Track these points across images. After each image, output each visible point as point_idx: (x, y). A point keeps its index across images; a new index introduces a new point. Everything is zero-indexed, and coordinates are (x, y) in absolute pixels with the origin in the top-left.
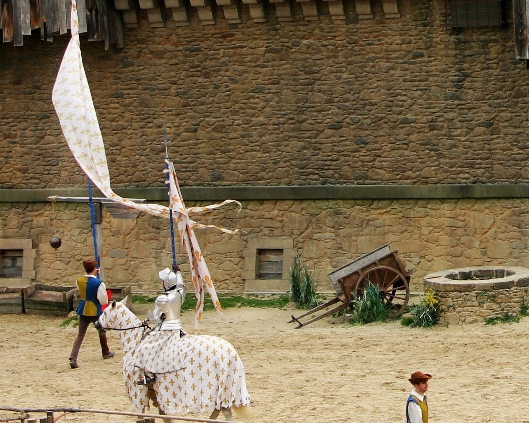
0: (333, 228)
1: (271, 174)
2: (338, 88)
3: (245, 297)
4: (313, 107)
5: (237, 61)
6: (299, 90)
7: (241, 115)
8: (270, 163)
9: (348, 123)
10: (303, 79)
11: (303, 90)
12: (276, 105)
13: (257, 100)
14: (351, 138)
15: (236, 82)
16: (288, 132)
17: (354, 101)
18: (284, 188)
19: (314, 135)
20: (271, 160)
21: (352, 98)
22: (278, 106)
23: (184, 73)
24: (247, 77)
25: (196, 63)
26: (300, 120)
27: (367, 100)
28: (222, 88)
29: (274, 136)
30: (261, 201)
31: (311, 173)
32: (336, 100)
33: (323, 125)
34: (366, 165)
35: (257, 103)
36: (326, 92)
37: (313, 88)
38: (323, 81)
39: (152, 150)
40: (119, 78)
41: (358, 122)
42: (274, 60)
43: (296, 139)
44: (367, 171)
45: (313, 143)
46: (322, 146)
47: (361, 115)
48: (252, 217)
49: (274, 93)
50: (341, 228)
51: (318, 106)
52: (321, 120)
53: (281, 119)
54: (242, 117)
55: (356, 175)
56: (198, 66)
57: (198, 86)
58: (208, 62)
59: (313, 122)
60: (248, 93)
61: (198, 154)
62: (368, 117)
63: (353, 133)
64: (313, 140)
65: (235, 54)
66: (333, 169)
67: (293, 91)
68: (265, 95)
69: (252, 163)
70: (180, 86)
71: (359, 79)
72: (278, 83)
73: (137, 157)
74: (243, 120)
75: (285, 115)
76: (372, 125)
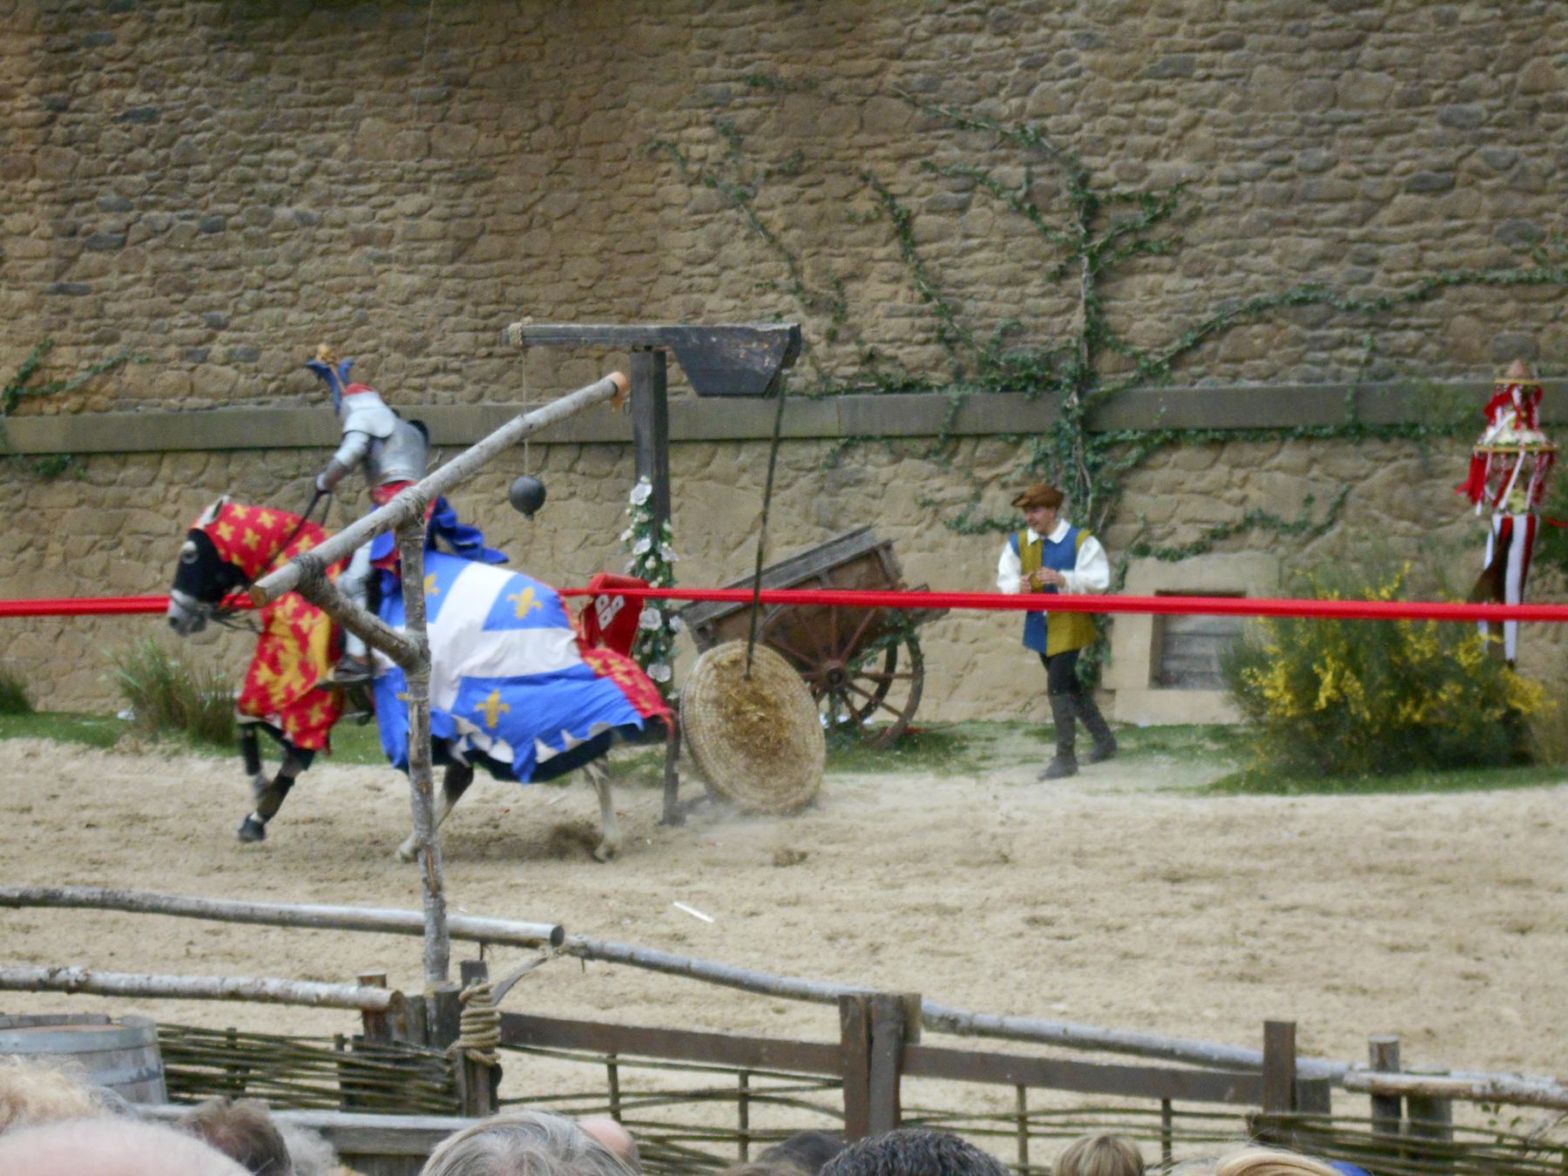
0: (1416, 520)
2: (1445, 56)
4: (1358, 121)
6: (1308, 67)
7: (1111, 153)
8: (1205, 311)
9: (1477, 173)
10: (1323, 29)
11: (1324, 63)
12: (1235, 117)
13: (1165, 104)
14: (1484, 220)
15: (1101, 46)
16: (1271, 206)
17: (1495, 95)
18: (1253, 392)
19: (1357, 216)
20: (1211, 299)
21: (1492, 86)
22: (1240, 122)
23: (927, 20)
24: (1135, 29)
26: (1313, 165)
27: (1541, 92)
28: (1052, 67)
29: (1220, 220)
31: (1341, 343)
32: (1437, 94)
33: (1388, 179)
34: (1534, 312)
35: (1166, 114)
36: (1401, 71)
37: (1358, 55)
38: (1392, 31)
40: (715, 45)
41: (1508, 168)
43: (1294, 230)
44: (1539, 330)
45: (1355, 242)
46: (1382, 252)
47: (1519, 143)
49: (1222, 78)
50: (1443, 519)
51: (1374, 117)
52: (1382, 161)
53: (1248, 166)
54: (1114, 158)
55: (1501, 345)
57: (972, 63)
59: (1354, 169)
60: (1137, 79)
61: (971, 283)
62: (1544, 152)
63: (1488, 204)
64: (1353, 232)
66: (1420, 328)
67: (1290, 68)
68: (1196, 85)
69: (1147, 310)
70: (914, 64)
71: (1516, 22)
72: (1238, 44)
74: (1119, 170)
75: (1260, 150)
76: (1559, 175)
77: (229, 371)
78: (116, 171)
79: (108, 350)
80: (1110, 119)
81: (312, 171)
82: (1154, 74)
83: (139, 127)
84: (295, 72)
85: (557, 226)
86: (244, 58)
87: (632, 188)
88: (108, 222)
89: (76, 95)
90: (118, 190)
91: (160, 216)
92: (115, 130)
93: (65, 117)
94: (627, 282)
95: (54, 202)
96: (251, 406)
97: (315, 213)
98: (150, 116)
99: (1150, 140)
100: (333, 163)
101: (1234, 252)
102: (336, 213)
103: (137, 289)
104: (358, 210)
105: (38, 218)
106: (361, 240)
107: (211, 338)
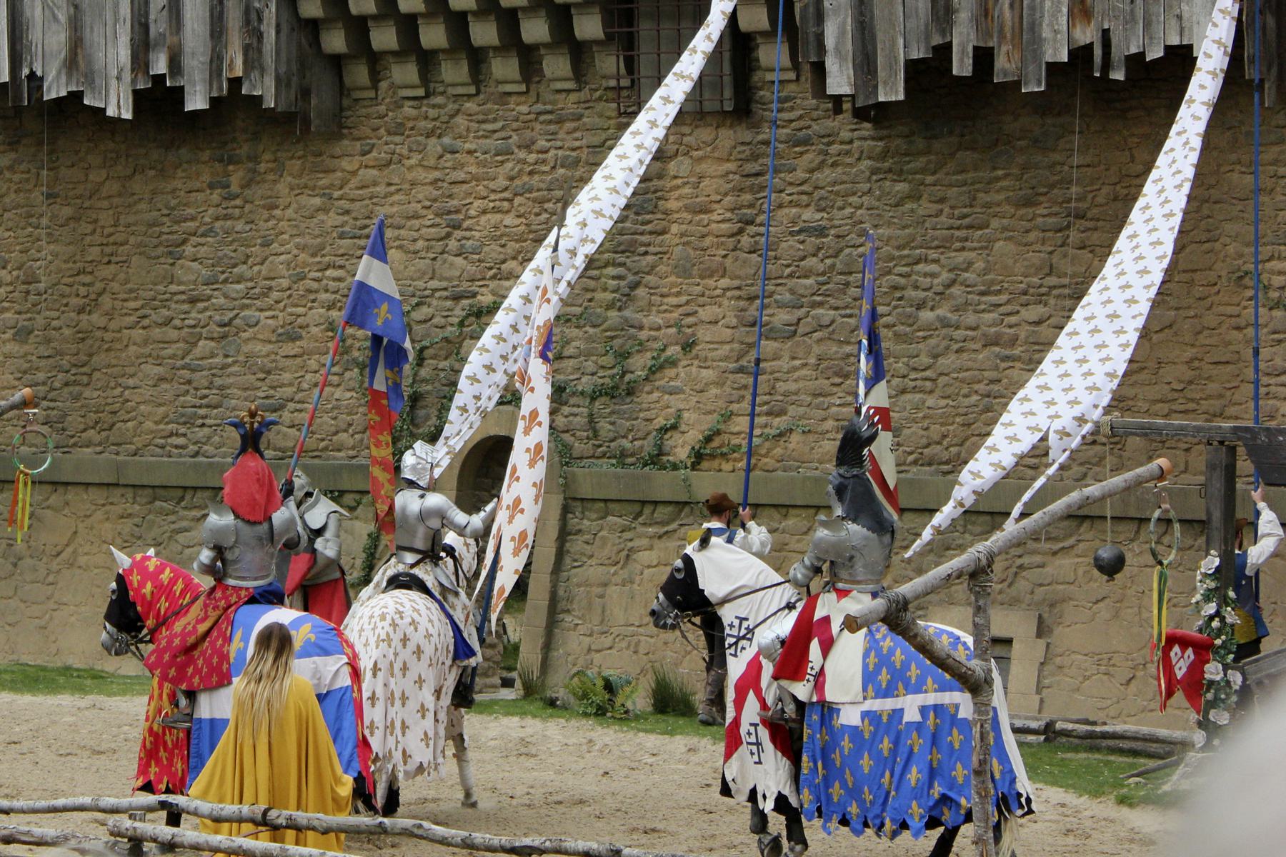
78: (791, 276)
81: (952, 283)
84: (942, 200)
85: (1155, 337)
86: (902, 187)
87: (1221, 309)
89: (761, 212)
90: (792, 291)
91: (825, 314)
92: (792, 241)
93: (752, 229)
94: (1213, 387)
95: (739, 298)
97: (953, 317)
98: (821, 232)
100: (969, 276)
102: (971, 318)
103: (804, 372)
105: (727, 310)
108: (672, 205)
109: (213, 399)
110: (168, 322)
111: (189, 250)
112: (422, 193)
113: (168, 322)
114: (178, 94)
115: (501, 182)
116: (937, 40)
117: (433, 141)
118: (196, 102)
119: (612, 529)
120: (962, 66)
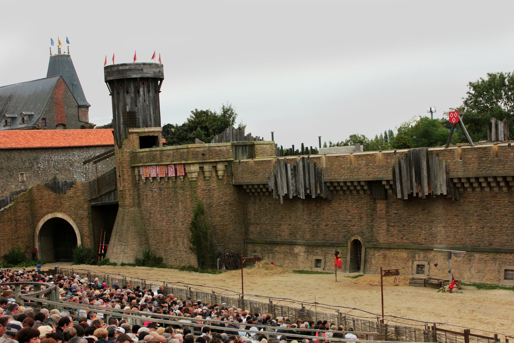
1: (509, 244)
3: (500, 286)
5: (498, 205)
13: (505, 219)
25: (484, 205)
28: (493, 214)
29: (511, 231)
30: (506, 253)
35: (505, 220)
39: (468, 234)
42: (511, 205)
48: (503, 258)
56: (484, 207)
58: (488, 205)
65: (497, 203)
73: (463, 236)
77: (406, 240)
79: (393, 237)
80: (499, 220)
81: (414, 220)
82: (504, 216)
83: (396, 215)
84: (413, 210)
86: (407, 208)
88: (393, 224)
91: (398, 224)
96: (408, 244)
97: (415, 225)
98: (397, 214)
99: (502, 222)
100: (416, 219)
101: (512, 234)
103: (396, 231)
104: (420, 225)
105: (385, 223)
106: (420, 228)
107: (403, 237)
108: (378, 210)
109: (317, 234)
110: (310, 224)
111: (312, 214)
112: (344, 208)
113: (310, 224)
114: (311, 196)
115: (355, 206)
116: (411, 192)
117: (345, 201)
118: (314, 197)
119: (372, 251)
120: (415, 195)
